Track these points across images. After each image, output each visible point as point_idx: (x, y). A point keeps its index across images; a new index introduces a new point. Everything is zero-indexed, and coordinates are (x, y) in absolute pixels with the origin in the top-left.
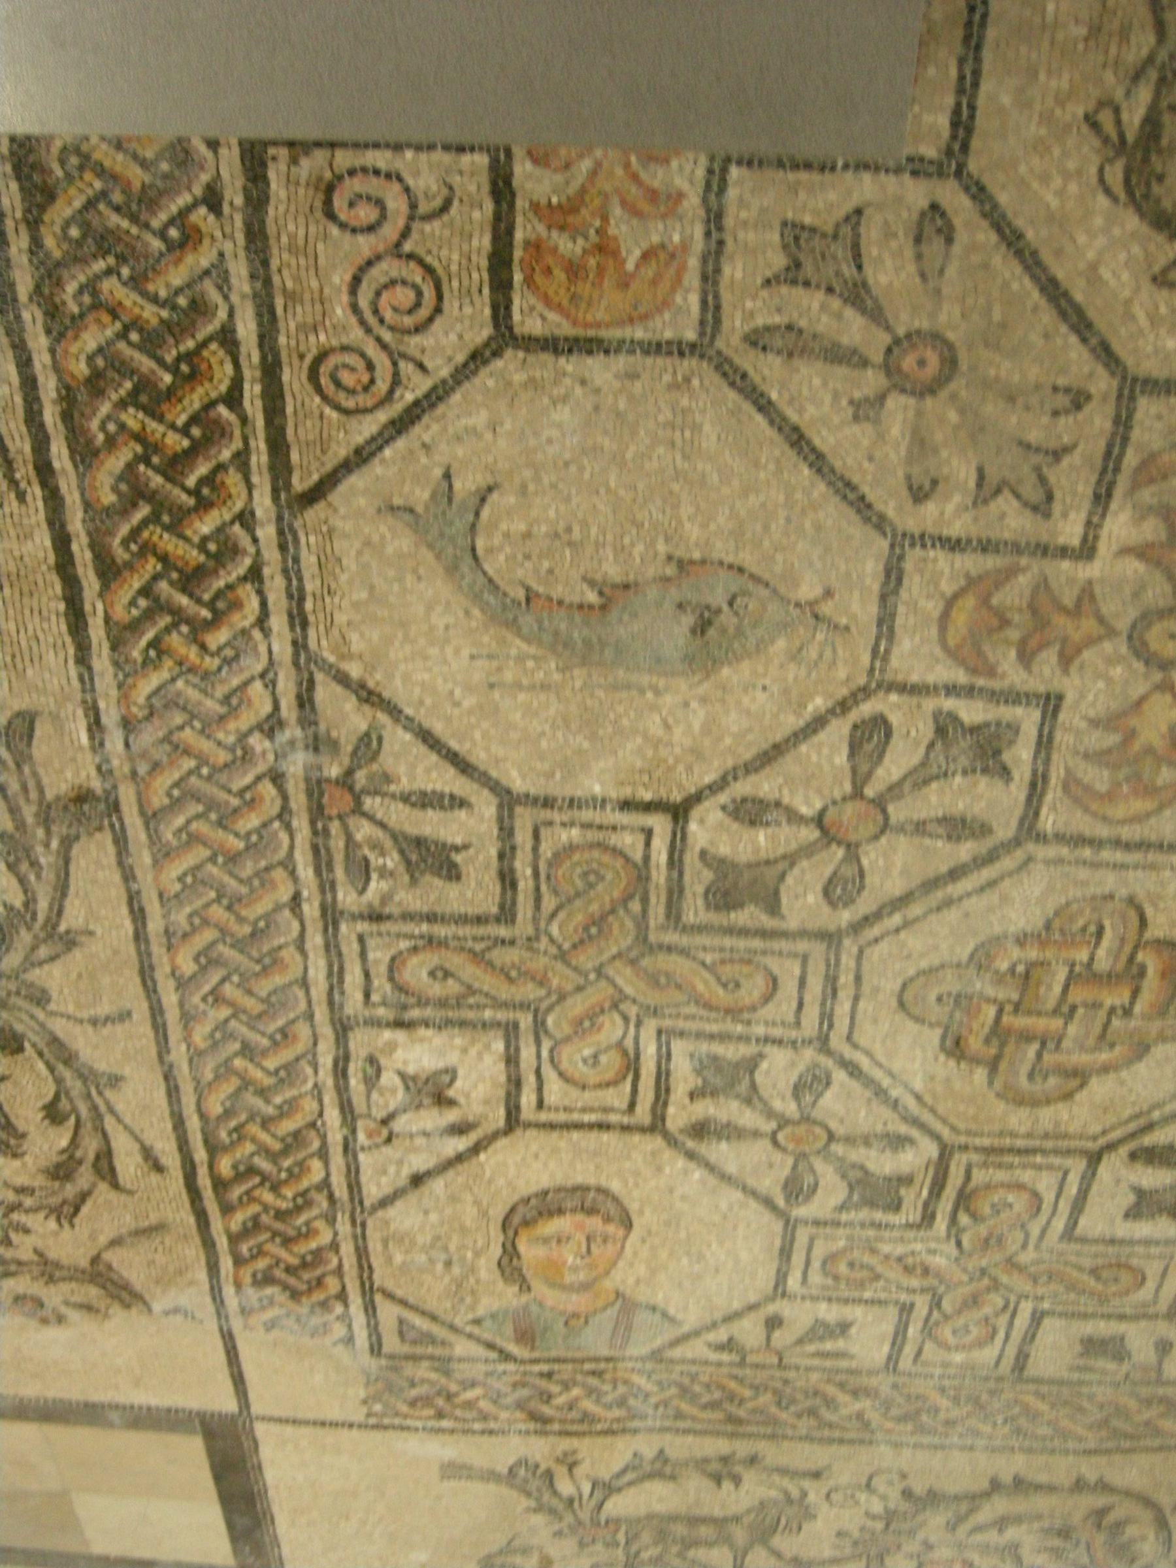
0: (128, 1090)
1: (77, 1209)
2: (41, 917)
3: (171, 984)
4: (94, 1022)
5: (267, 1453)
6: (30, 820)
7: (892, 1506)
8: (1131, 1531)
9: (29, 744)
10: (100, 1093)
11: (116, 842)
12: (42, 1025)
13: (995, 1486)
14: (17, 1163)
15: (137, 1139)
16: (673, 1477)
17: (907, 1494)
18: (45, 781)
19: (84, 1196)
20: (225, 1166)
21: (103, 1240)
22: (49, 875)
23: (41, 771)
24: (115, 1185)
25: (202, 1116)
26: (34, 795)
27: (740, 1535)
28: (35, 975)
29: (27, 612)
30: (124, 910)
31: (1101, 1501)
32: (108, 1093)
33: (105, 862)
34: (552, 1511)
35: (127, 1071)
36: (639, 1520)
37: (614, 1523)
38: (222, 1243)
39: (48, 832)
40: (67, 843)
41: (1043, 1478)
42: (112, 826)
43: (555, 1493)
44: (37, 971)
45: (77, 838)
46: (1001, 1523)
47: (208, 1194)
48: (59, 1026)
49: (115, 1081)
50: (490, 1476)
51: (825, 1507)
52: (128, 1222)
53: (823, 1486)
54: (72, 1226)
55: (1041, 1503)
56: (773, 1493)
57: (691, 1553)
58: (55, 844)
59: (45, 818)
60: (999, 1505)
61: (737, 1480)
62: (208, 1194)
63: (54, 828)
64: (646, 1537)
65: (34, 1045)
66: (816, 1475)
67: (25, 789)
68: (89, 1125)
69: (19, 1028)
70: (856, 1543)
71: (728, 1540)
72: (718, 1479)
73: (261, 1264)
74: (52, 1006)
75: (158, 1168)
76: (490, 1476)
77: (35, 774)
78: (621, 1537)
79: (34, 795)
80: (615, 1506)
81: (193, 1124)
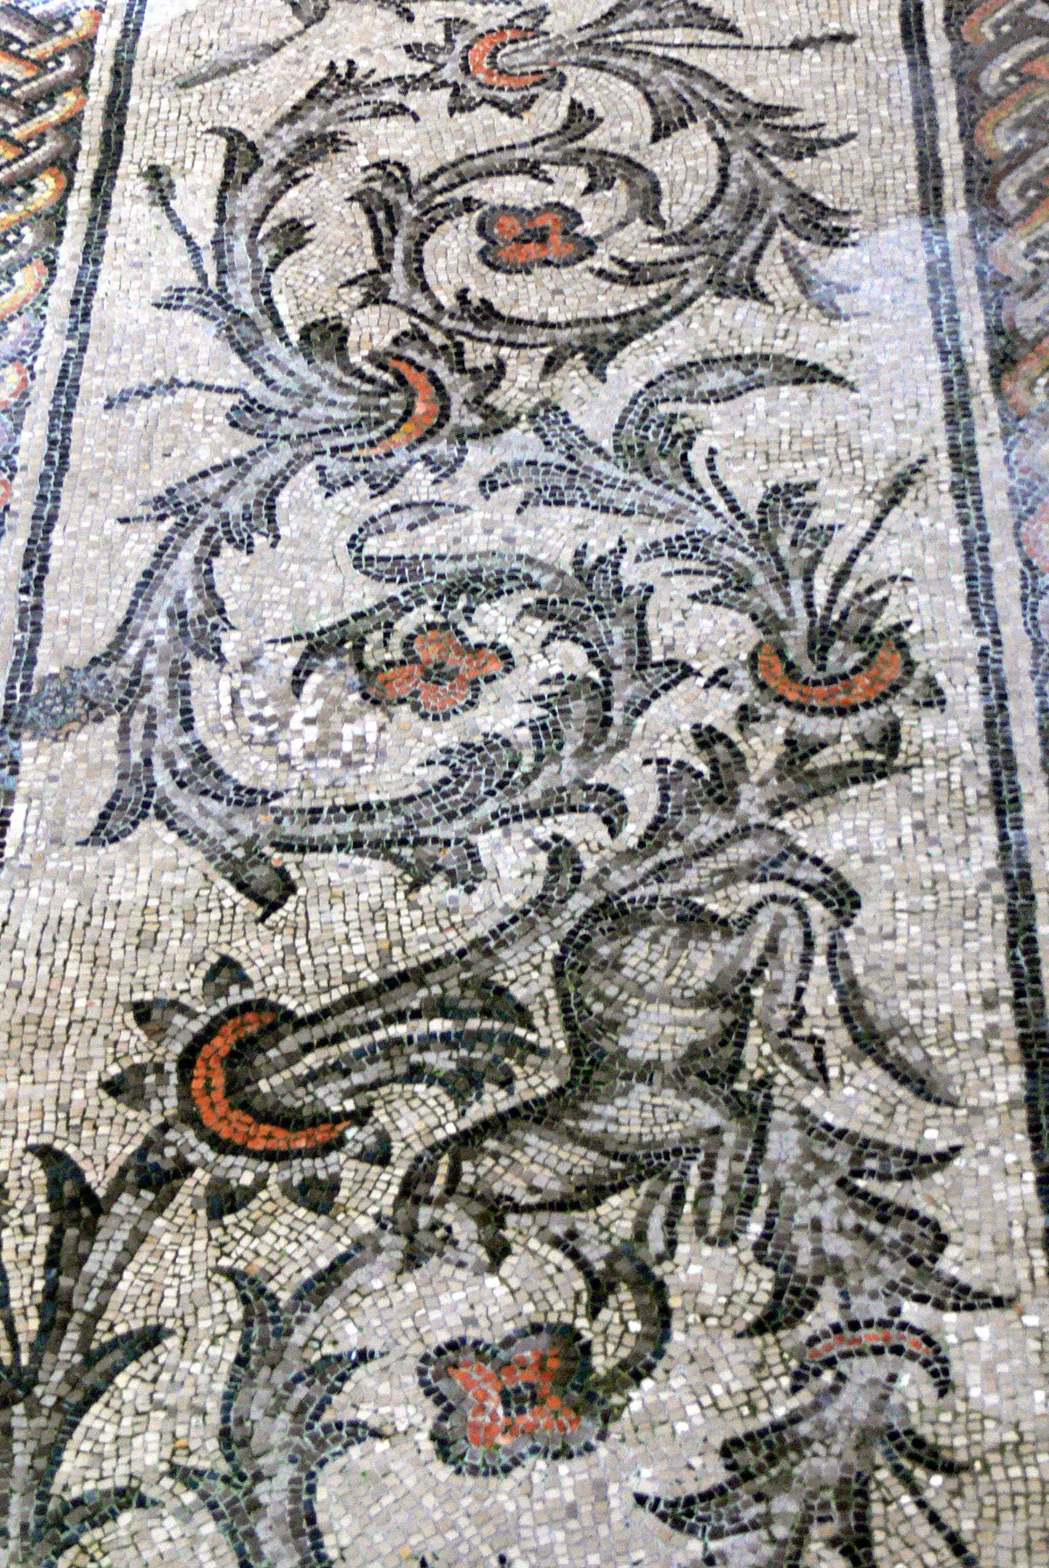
0: (158, 287)
1: (311, 95)
2: (199, 533)
3: (19, 460)
4: (173, 385)
6: (160, 684)
9: (117, 795)
10: (203, 278)
11: (32, 662)
12: (258, 371)
14: (383, 153)
15: (170, 213)
18: (110, 744)
19: (294, 115)
20: (46, 187)
21: (289, 52)
22: (162, 601)
23: (113, 758)
24: (234, 138)
25: (51, 265)
26: (139, 719)
28: (241, 445)
29: (40, 994)
30: (52, 564)
32: (191, 278)
33: (61, 632)
35: (146, 316)
38: (100, 76)
39: (139, 665)
40: (114, 653)
42: (25, 687)
44: (235, 453)
45: (95, 661)
47: (90, 143)
48: (235, 372)
49: (174, 300)
52: (234, 84)
54: (332, 67)
58: (134, 649)
59: (137, 683)
62: (90, 143)
63: (126, 673)
65: (284, 338)
67: (150, 728)
68: (240, 226)
69: (298, 364)
73: (46, 48)
74: (229, 401)
75: (155, 173)
77: (125, 752)
79: (139, 719)
81: (69, 251)
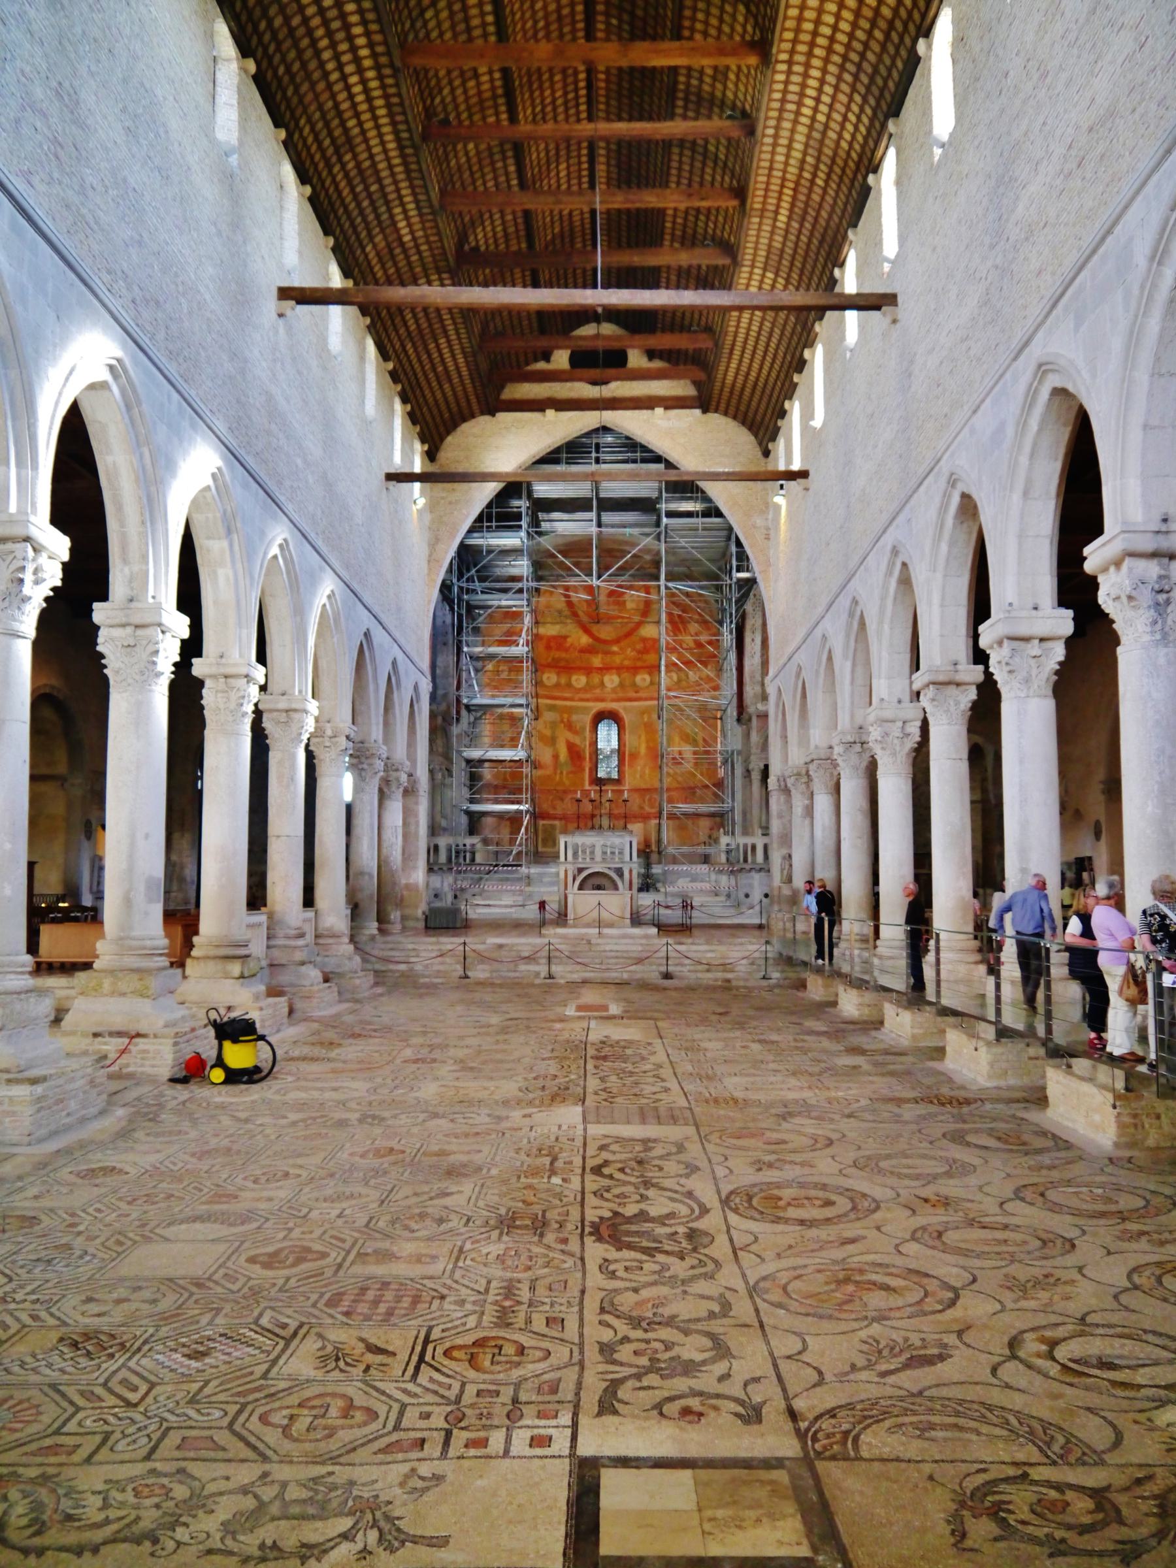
5: (560, 1547)
7: (170, 1533)
8: (24, 1521)
13: (95, 1550)
16: (304, 1545)
17: (155, 1541)
27: (275, 1509)
31: (37, 1541)
34: (388, 1518)
36: (336, 1516)
37: (351, 1513)
41: (64, 1555)
43: (380, 1530)
46: (107, 1522)
50: (415, 1540)
51: (212, 1531)
53: (210, 1544)
55: (72, 1538)
56: (241, 1538)
57: (311, 1494)
60: (98, 1536)
61: (262, 1546)
64: (334, 1504)
66: (210, 1552)
70: (204, 1505)
71: (285, 1504)
72: (275, 1546)
76: (415, 1540)
78: (350, 1503)
80: (345, 1524)
